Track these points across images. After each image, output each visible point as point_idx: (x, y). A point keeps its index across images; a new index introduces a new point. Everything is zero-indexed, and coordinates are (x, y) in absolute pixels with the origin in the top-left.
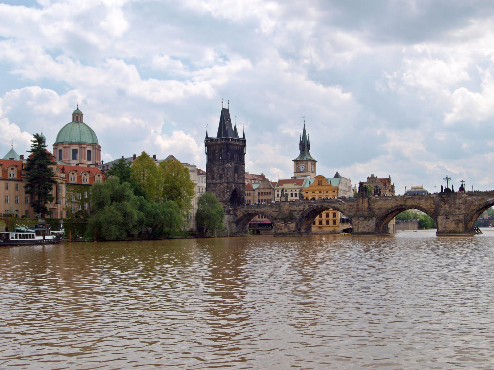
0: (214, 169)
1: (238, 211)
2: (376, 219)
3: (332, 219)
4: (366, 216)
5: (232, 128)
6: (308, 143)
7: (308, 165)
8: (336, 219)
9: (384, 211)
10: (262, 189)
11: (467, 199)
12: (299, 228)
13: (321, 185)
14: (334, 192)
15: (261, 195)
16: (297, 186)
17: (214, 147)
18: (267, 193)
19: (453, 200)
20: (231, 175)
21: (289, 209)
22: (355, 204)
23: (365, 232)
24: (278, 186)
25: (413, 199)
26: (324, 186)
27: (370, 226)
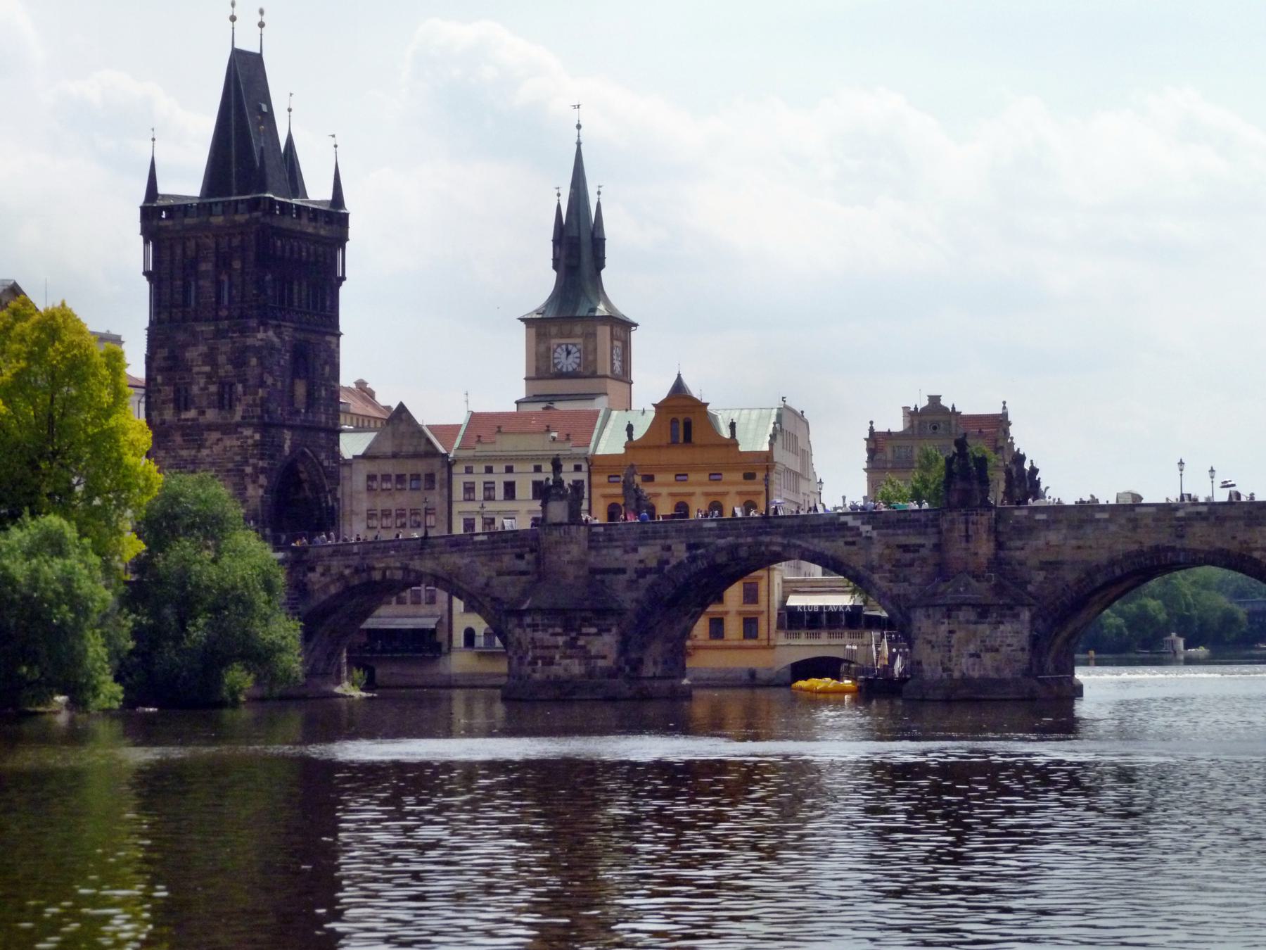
0: (188, 355)
1: (312, 569)
2: (1033, 619)
6: (596, 236)
9: (1070, 576)
10: (385, 457)
12: (633, 655)
13: (688, 438)
14: (749, 476)
17: (191, 244)
18: (416, 477)
20: (279, 384)
21: (582, 563)
23: (981, 678)
25: (1217, 518)
27: (1004, 649)
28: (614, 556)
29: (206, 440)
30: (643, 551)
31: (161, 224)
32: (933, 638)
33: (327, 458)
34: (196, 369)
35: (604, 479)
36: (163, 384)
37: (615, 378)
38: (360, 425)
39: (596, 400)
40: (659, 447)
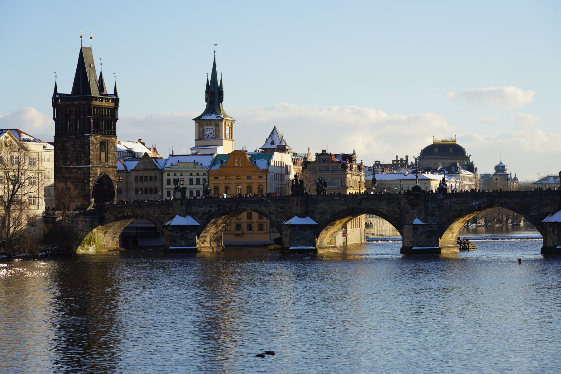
1: (106, 212)
3: (257, 222)
5: (96, 76)
6: (220, 90)
8: (263, 222)
10: (141, 170)
11: (444, 201)
14: (260, 177)
15: (140, 181)
17: (68, 110)
18: (151, 177)
19: (424, 203)
20: (96, 154)
27: (308, 238)
29: (73, 171)
30: (204, 208)
31: (58, 103)
32: (286, 234)
33: (112, 176)
34: (69, 149)
35: (213, 178)
39: (218, 148)
40: (231, 167)
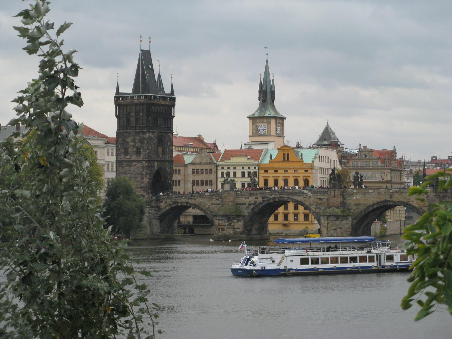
0: (128, 140)
1: (162, 202)
3: (303, 213)
4: (339, 215)
7: (270, 124)
9: (362, 208)
12: (248, 228)
13: (288, 159)
14: (306, 171)
16: (251, 162)
17: (129, 108)
20: (153, 149)
21: (234, 202)
22: (325, 197)
24: (222, 160)
26: (292, 162)
27: (344, 228)
28: (242, 200)
31: (120, 101)
32: (324, 225)
33: (169, 169)
34: (130, 144)
35: (263, 171)
36: (120, 148)
37: (277, 136)
38: (196, 151)
